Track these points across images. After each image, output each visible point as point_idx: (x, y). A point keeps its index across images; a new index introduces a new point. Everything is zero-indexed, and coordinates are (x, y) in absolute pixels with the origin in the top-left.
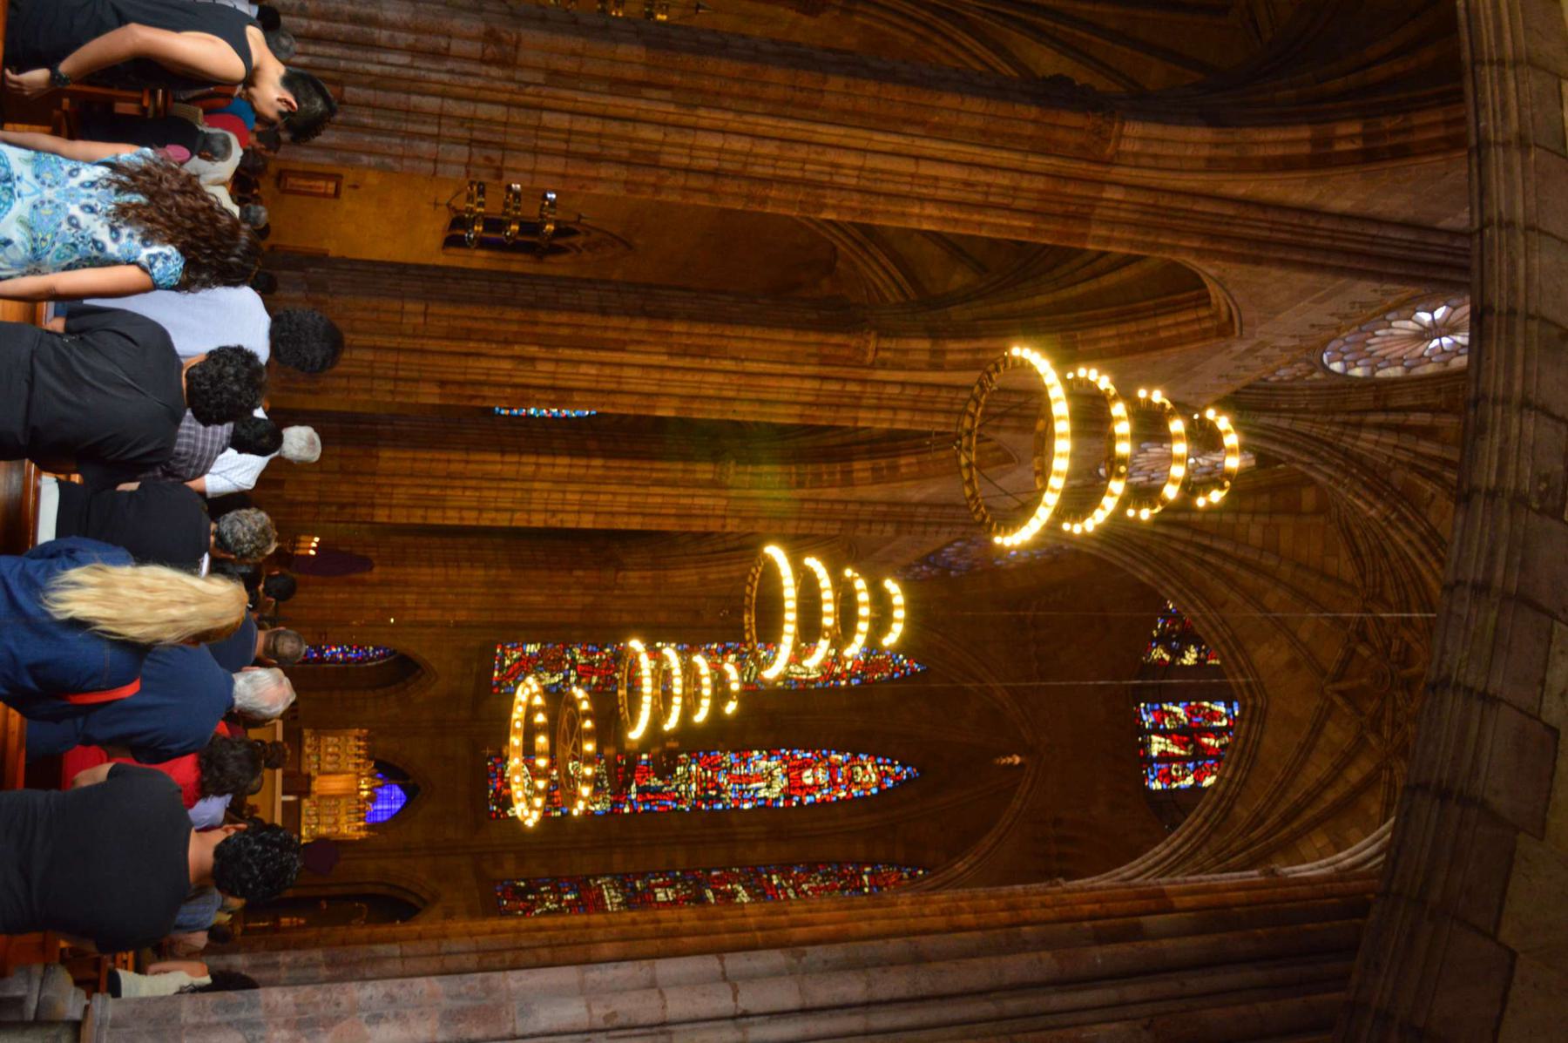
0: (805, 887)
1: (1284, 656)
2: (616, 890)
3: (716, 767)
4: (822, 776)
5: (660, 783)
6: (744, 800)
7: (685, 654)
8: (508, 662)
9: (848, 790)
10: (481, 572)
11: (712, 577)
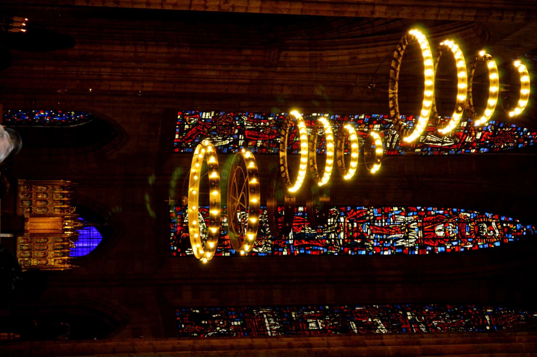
0: (435, 323)
3: (361, 220)
4: (453, 230)
5: (313, 231)
7: (338, 123)
8: (187, 127)
9: (475, 243)
10: (165, 50)
11: (361, 57)
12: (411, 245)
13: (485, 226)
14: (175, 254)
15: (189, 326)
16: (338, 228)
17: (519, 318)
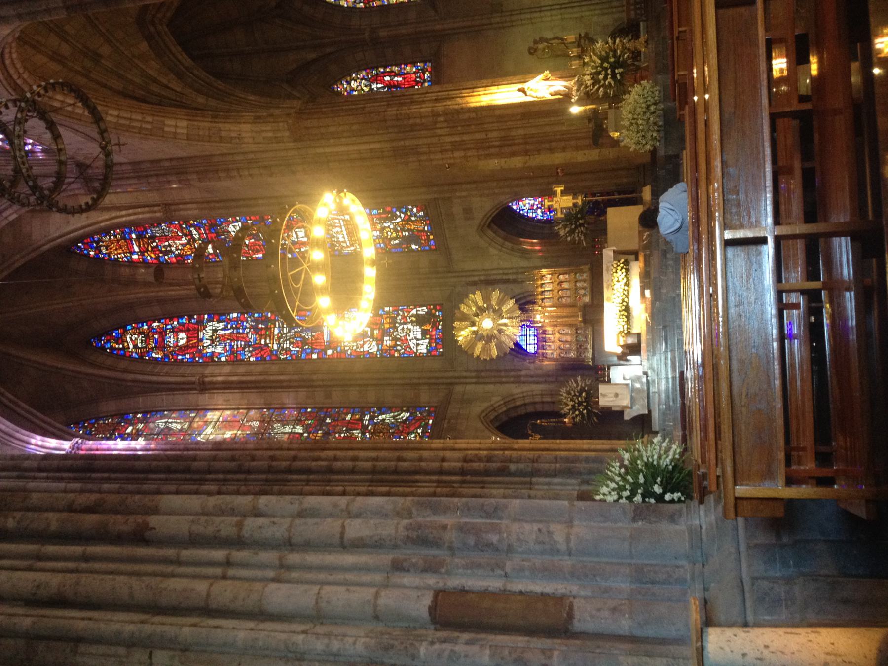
0: (184, 240)
2: (338, 242)
3: (258, 348)
4: (171, 340)
5: (303, 334)
6: (237, 320)
8: (420, 431)
9: (150, 328)
12: (211, 323)
13: (139, 345)
14: (438, 307)
15: (421, 228)
16: (279, 338)
17: (107, 249)
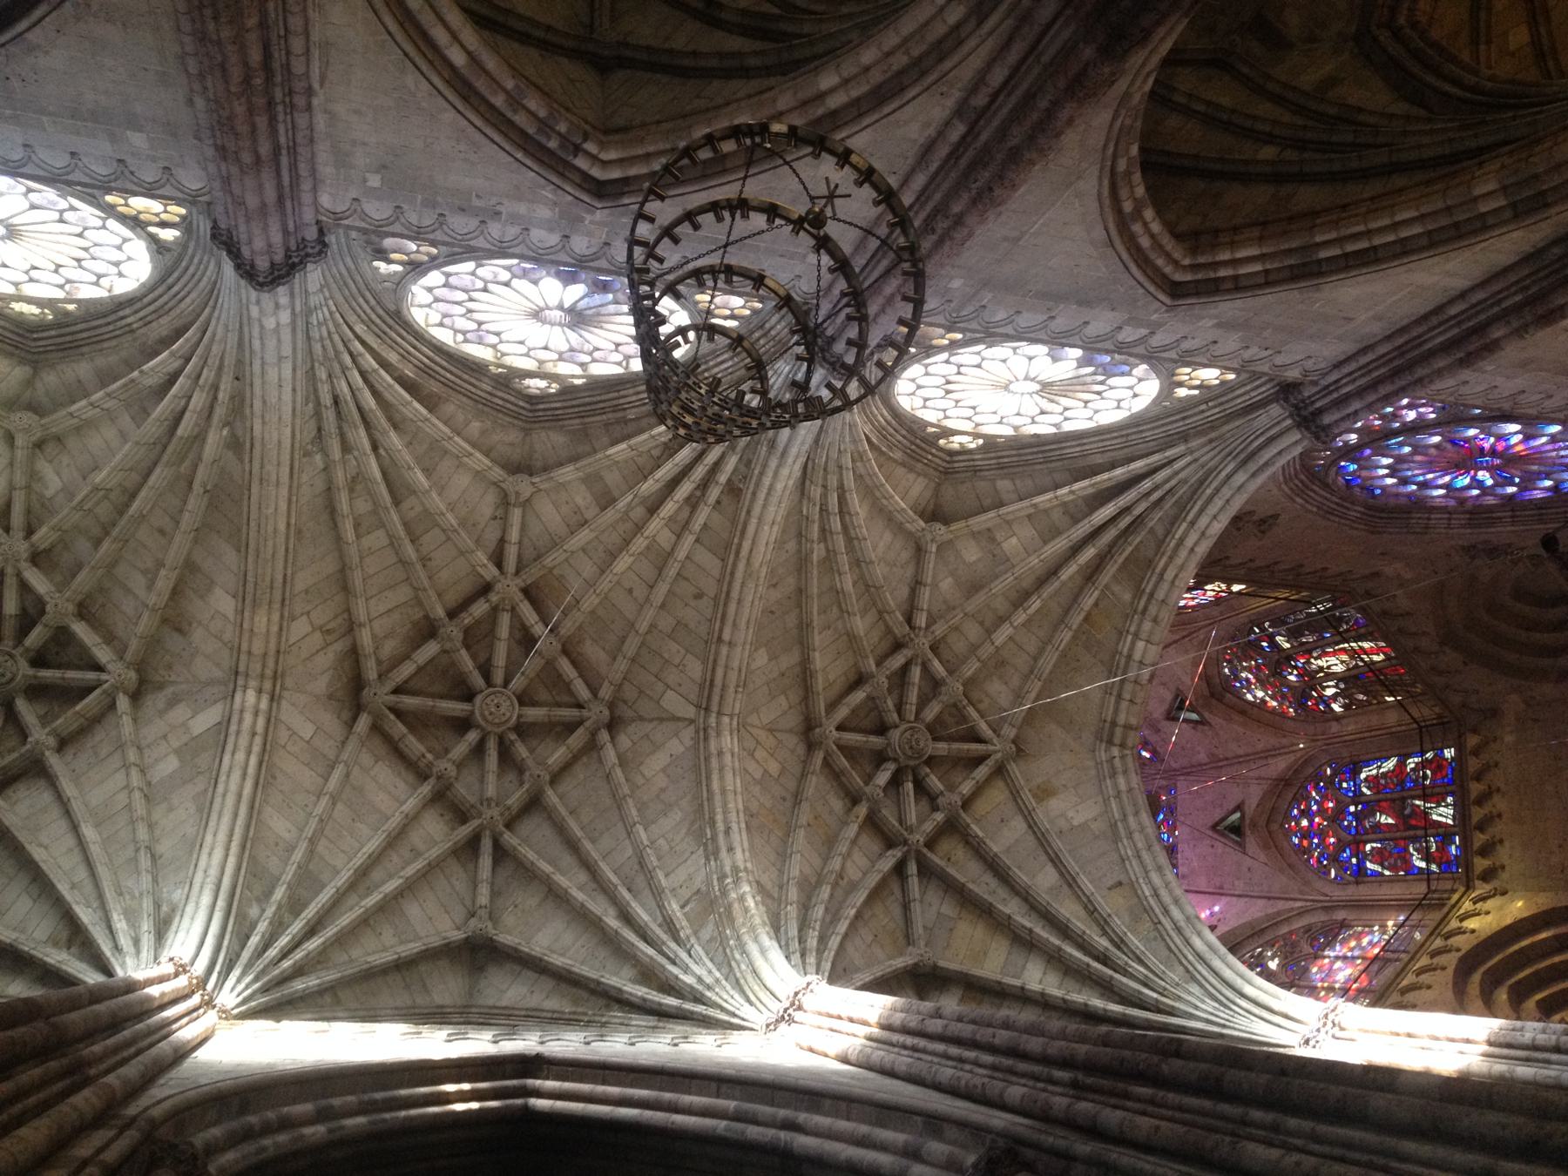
1: (1055, 804)
